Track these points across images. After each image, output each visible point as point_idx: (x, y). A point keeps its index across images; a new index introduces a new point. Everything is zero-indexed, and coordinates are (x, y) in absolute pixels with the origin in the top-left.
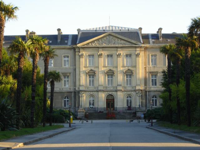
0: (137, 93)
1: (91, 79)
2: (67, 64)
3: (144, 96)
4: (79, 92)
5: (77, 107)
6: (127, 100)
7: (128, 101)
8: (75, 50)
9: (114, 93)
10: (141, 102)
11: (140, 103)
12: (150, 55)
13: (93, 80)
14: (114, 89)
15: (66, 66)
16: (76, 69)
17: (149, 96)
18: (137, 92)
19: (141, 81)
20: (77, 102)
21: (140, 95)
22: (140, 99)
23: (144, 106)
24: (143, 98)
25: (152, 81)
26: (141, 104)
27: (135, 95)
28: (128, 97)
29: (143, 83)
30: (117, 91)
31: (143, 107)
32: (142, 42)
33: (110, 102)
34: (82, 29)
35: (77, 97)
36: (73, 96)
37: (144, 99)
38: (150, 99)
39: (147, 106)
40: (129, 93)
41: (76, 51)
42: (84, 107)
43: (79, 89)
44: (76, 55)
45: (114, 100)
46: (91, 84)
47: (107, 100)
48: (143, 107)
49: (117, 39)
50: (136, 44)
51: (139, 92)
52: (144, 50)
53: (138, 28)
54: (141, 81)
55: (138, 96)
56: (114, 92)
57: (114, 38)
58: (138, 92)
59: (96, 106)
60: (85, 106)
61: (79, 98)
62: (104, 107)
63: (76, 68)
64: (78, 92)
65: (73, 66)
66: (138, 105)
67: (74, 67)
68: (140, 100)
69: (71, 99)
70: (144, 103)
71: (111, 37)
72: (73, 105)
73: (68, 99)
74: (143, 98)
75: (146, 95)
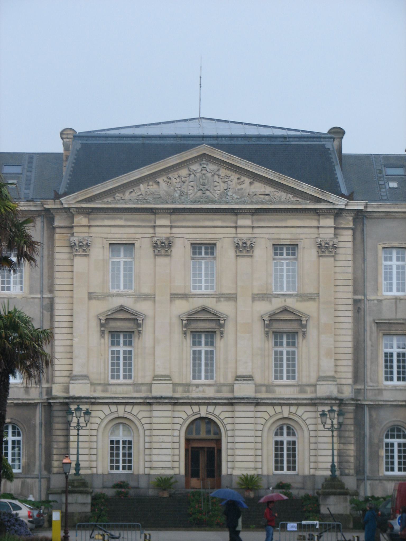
0: (323, 414)
1: (121, 348)
2: (15, 283)
3: (352, 428)
4: (67, 404)
5: (55, 470)
6: (276, 443)
7: (279, 445)
8: (51, 220)
9: (220, 414)
10: (339, 456)
11: (336, 459)
12: (380, 247)
13: (130, 352)
14: (219, 395)
15: (9, 289)
16: (57, 306)
17: (372, 426)
18: (321, 408)
19: (339, 363)
20: (55, 451)
21: (335, 421)
22: (335, 440)
23: (352, 472)
24: (347, 434)
25: (386, 361)
26: (340, 462)
27: (313, 421)
28: (281, 428)
29: (345, 369)
30: (232, 404)
31: (348, 475)
32: (344, 190)
33: (204, 452)
34: (80, 129)
35: (58, 426)
36: (41, 424)
37: (353, 440)
38: (376, 441)
39: (364, 473)
40: (286, 411)
41: (56, 224)
42: (89, 472)
43: (67, 390)
44: (57, 243)
45: (219, 441)
46: (118, 371)
47: (188, 441)
48: (348, 475)
49: (234, 176)
50: (319, 200)
51: (332, 411)
52: (351, 225)
53: (326, 132)
54: (339, 363)
55: (329, 426)
56: (218, 410)
57: (223, 172)
58: (327, 409)
59: (140, 466)
60: (91, 468)
61: (68, 430)
62: (177, 471)
63: (57, 300)
64: (62, 404)
65: (42, 292)
66: (329, 465)
67: (47, 295)
68: (336, 446)
69: (31, 439)
70: (352, 459)
71: (211, 167)
72: (39, 463)
73: (19, 435)
74: (347, 434)
75: (359, 424)
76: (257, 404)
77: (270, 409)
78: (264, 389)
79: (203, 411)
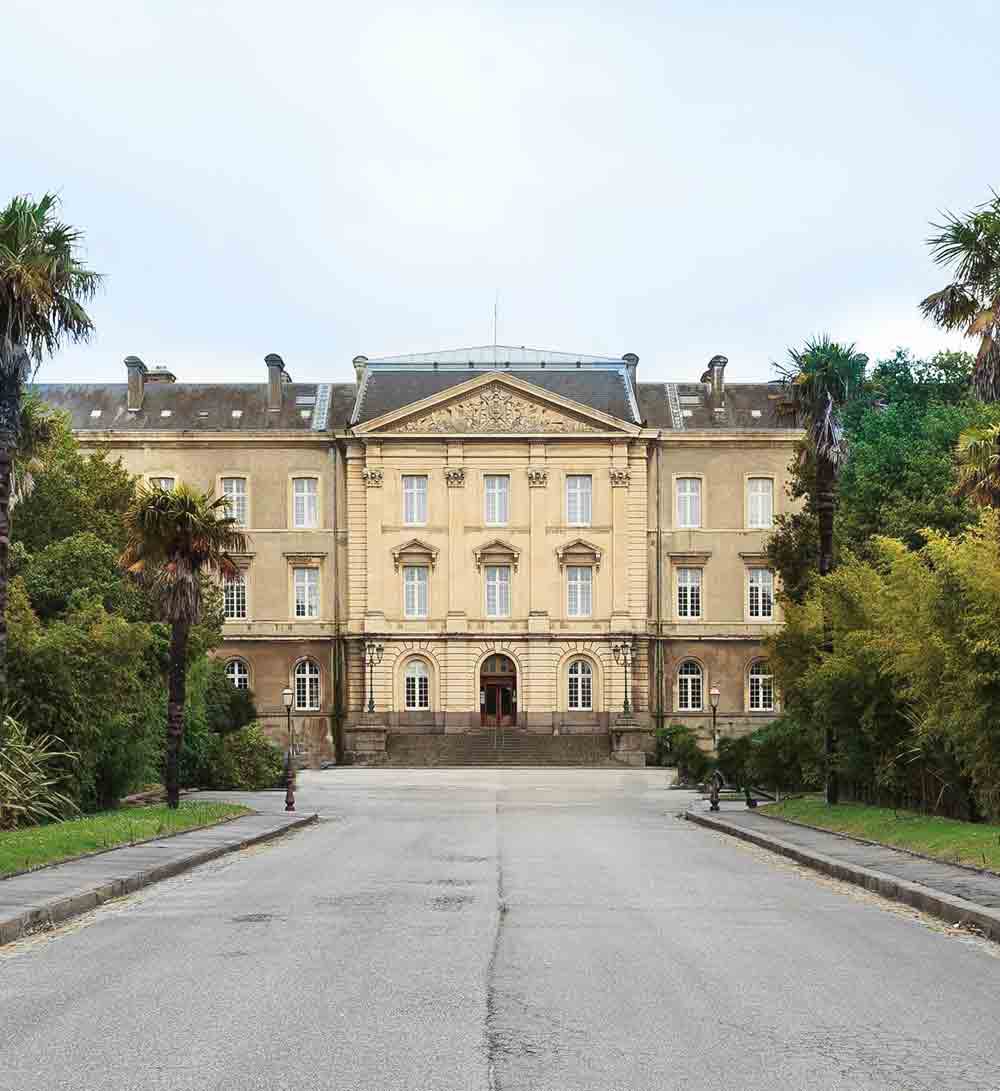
0: (616, 650)
6: (571, 680)
7: (573, 683)
8: (343, 453)
9: (514, 650)
11: (629, 695)
12: (674, 477)
14: (513, 632)
18: (614, 644)
20: (351, 689)
21: (629, 657)
22: (629, 676)
28: (576, 664)
30: (527, 640)
32: (637, 418)
33: (499, 686)
34: (372, 357)
40: (580, 647)
41: (348, 455)
42: (385, 710)
43: (363, 626)
44: (349, 475)
45: (514, 678)
47: (483, 678)
49: (526, 404)
50: (612, 429)
52: (645, 455)
53: (620, 357)
56: (514, 645)
57: (515, 400)
58: (620, 644)
59: (435, 704)
61: (364, 667)
62: (472, 709)
68: (629, 682)
71: (503, 394)
76: (552, 640)
77: (564, 645)
78: (558, 624)
79: (498, 648)
